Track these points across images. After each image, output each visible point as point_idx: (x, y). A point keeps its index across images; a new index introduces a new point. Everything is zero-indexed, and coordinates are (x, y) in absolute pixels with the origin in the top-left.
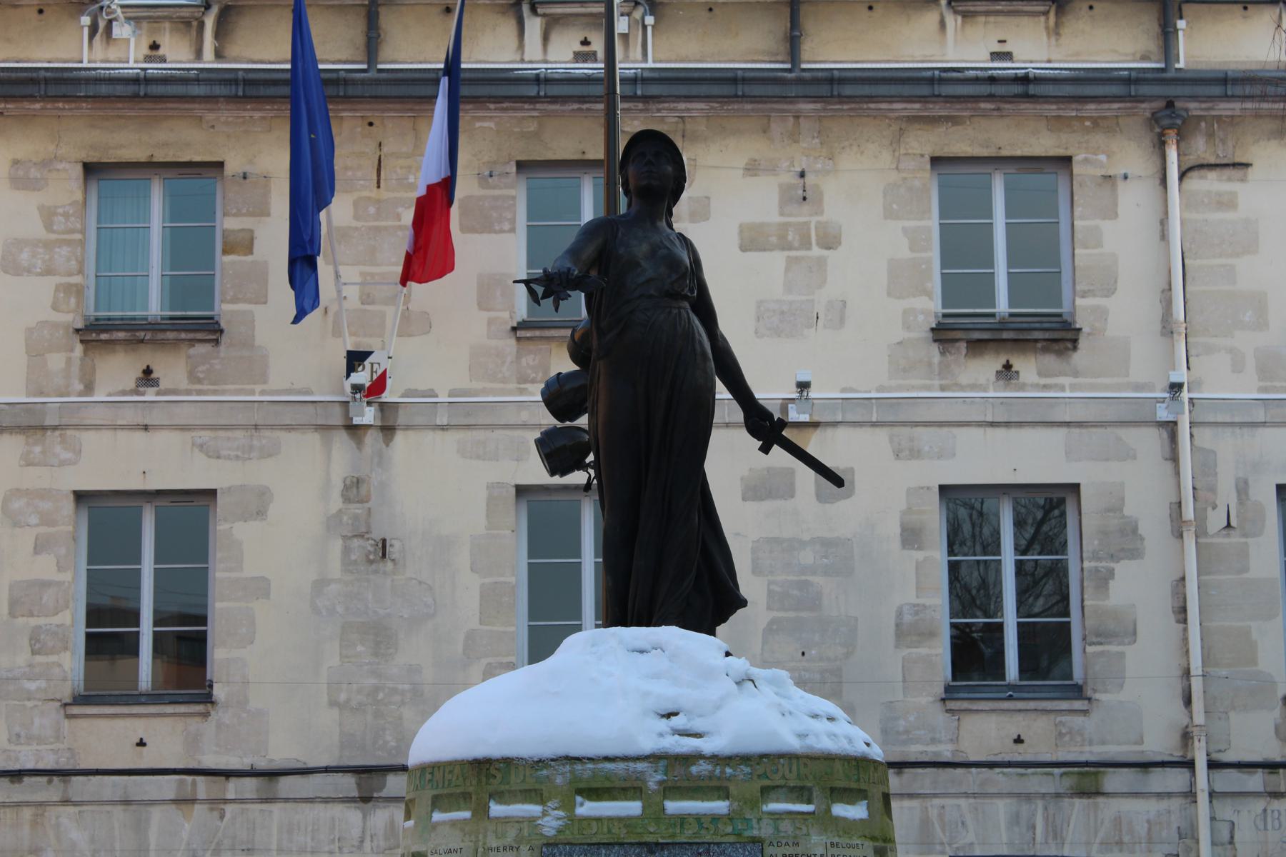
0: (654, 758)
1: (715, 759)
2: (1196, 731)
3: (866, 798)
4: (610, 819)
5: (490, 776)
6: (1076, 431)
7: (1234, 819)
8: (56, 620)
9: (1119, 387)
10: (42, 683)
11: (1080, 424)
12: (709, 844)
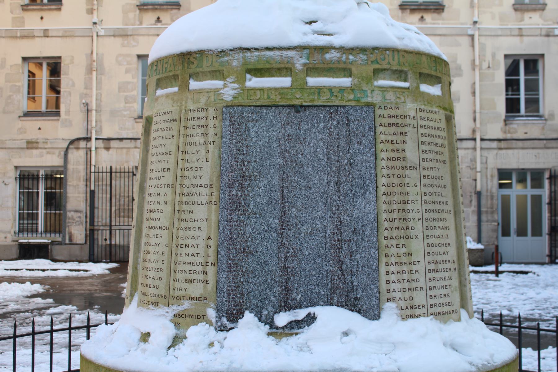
0: (300, 48)
1: (341, 49)
2: (477, 130)
3: (440, 82)
4: (270, 89)
5: (190, 63)
6: (443, 38)
7: (488, 156)
8: (132, 93)
9: (456, 24)
10: (128, 112)
11: (444, 35)
12: (338, 106)
